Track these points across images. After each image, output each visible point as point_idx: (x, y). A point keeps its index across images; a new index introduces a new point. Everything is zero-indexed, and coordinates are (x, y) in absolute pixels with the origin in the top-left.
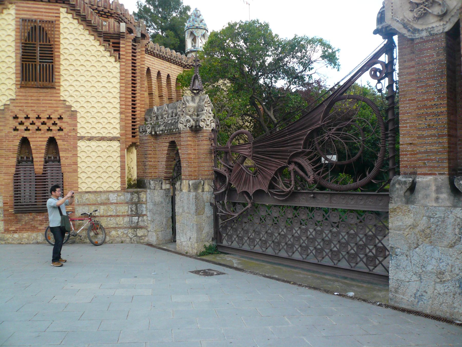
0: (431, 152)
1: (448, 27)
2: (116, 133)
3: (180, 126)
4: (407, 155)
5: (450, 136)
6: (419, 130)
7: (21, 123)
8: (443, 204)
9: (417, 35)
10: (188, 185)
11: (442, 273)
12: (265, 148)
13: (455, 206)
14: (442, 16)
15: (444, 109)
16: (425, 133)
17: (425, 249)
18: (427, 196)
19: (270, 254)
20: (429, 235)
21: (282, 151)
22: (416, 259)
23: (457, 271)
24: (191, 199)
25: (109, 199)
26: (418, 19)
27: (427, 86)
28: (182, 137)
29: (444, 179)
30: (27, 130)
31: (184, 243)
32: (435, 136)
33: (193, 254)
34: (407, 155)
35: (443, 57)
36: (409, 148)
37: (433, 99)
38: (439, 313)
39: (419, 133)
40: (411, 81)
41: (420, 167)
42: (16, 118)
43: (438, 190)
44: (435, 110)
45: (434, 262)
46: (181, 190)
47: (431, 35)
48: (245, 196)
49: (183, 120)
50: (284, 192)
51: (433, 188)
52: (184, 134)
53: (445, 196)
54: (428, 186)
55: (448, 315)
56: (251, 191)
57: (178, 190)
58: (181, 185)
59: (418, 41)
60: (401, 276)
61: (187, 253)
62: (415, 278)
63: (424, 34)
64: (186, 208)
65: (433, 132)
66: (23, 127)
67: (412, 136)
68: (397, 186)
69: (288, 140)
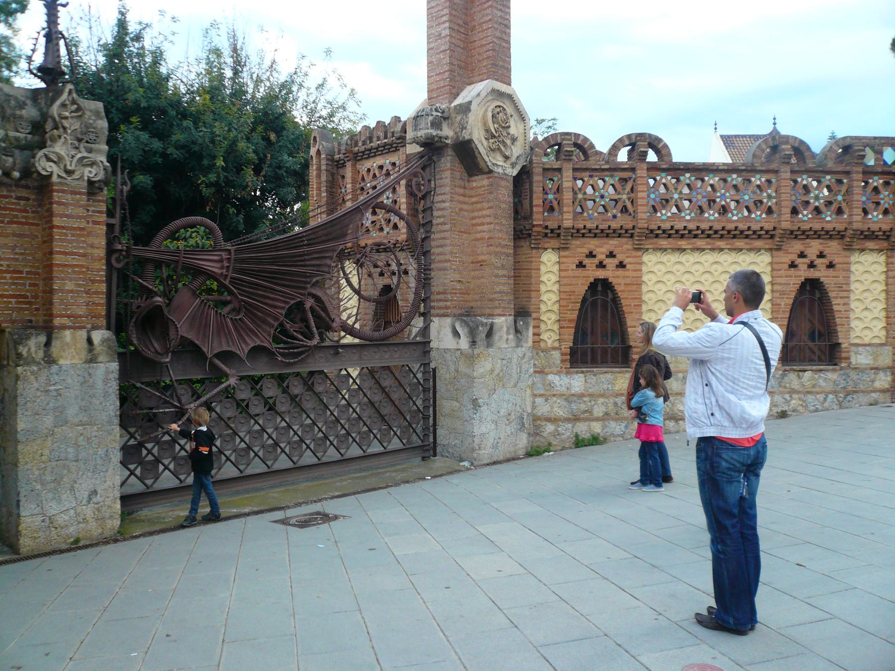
0: (504, 292)
1: (515, 172)
3: (43, 166)
4: (456, 293)
6: (497, 268)
8: (510, 345)
10: (85, 344)
11: (509, 415)
12: (262, 263)
13: (517, 346)
14: (507, 158)
16: (500, 272)
17: (500, 391)
18: (501, 337)
19: (258, 471)
20: (501, 379)
21: (290, 273)
23: (518, 409)
24: (100, 384)
26: (492, 150)
27: (501, 224)
28: (60, 203)
29: (512, 318)
31: (61, 519)
32: (505, 276)
33: (108, 534)
34: (456, 293)
36: (458, 286)
37: (505, 239)
38: (508, 456)
39: (496, 271)
40: (461, 210)
41: (496, 308)
43: (508, 333)
45: (505, 405)
46: (50, 360)
47: (505, 174)
48: (217, 362)
49: (62, 153)
50: (306, 346)
51: (505, 329)
52: (69, 196)
53: (511, 337)
54: (502, 327)
55: (513, 455)
56: (242, 350)
58: (48, 344)
59: (496, 175)
60: (484, 429)
61: (77, 541)
62: (493, 426)
63: (500, 170)
64: (72, 412)
65: (505, 272)
67: (460, 274)
68: (481, 328)
69: (305, 255)
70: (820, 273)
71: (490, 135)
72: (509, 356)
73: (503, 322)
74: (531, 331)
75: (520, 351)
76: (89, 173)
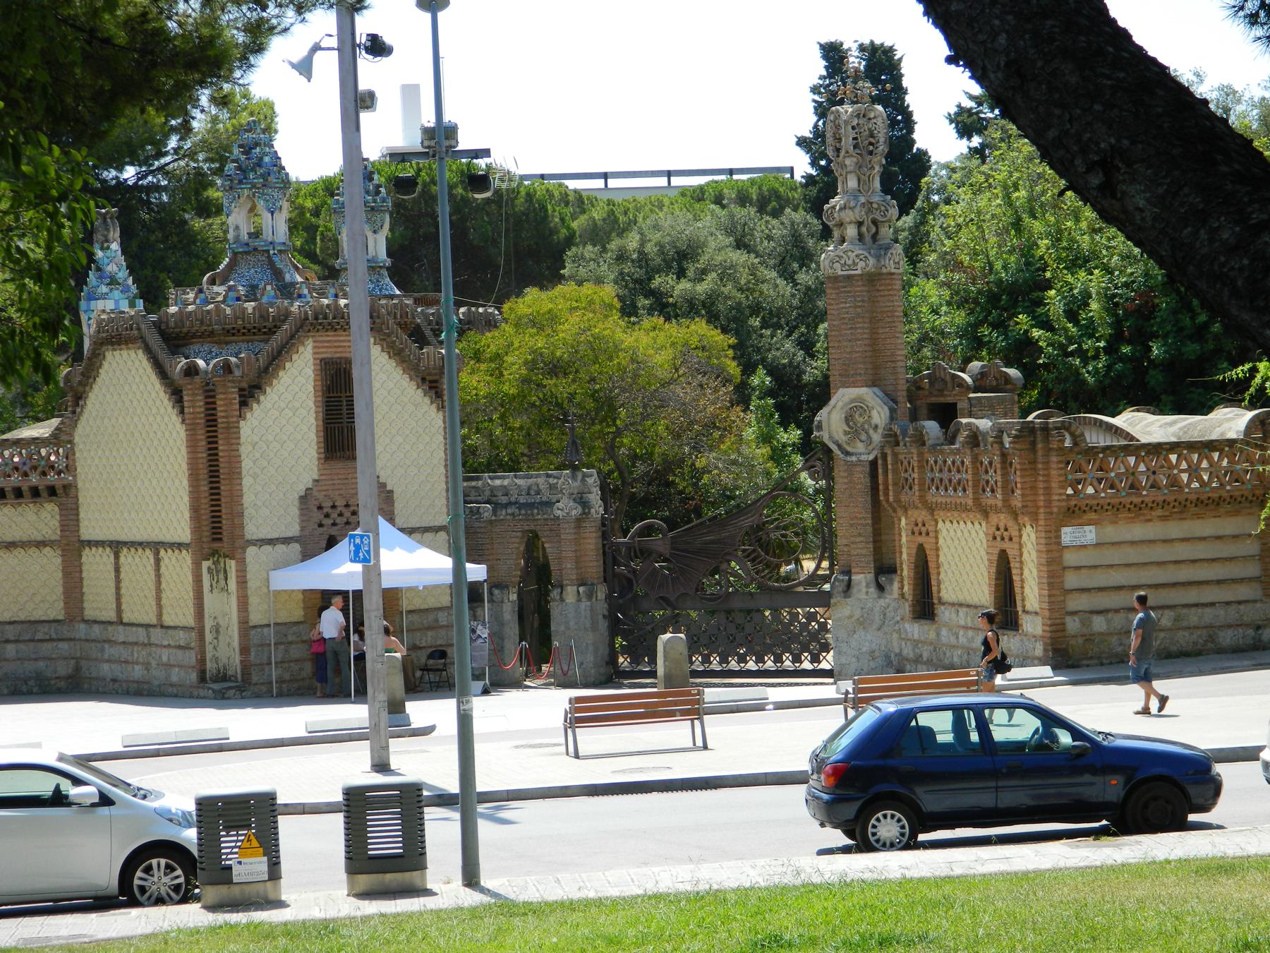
1: (871, 457)
2: (443, 519)
5: (874, 542)
7: (327, 516)
9: (849, 459)
15: (870, 522)
16: (858, 539)
18: (860, 591)
20: (863, 623)
22: (854, 644)
25: (437, 621)
29: (871, 576)
30: (334, 524)
35: (868, 480)
42: (320, 508)
43: (867, 586)
44: (863, 521)
46: (562, 600)
53: (872, 590)
54: (860, 583)
57: (554, 600)
62: (854, 660)
63: (854, 459)
64: (572, 624)
66: (329, 521)
70: (1006, 545)
71: (846, 433)
72: (870, 605)
73: (862, 579)
74: (896, 585)
75: (882, 602)
76: (574, 512)
